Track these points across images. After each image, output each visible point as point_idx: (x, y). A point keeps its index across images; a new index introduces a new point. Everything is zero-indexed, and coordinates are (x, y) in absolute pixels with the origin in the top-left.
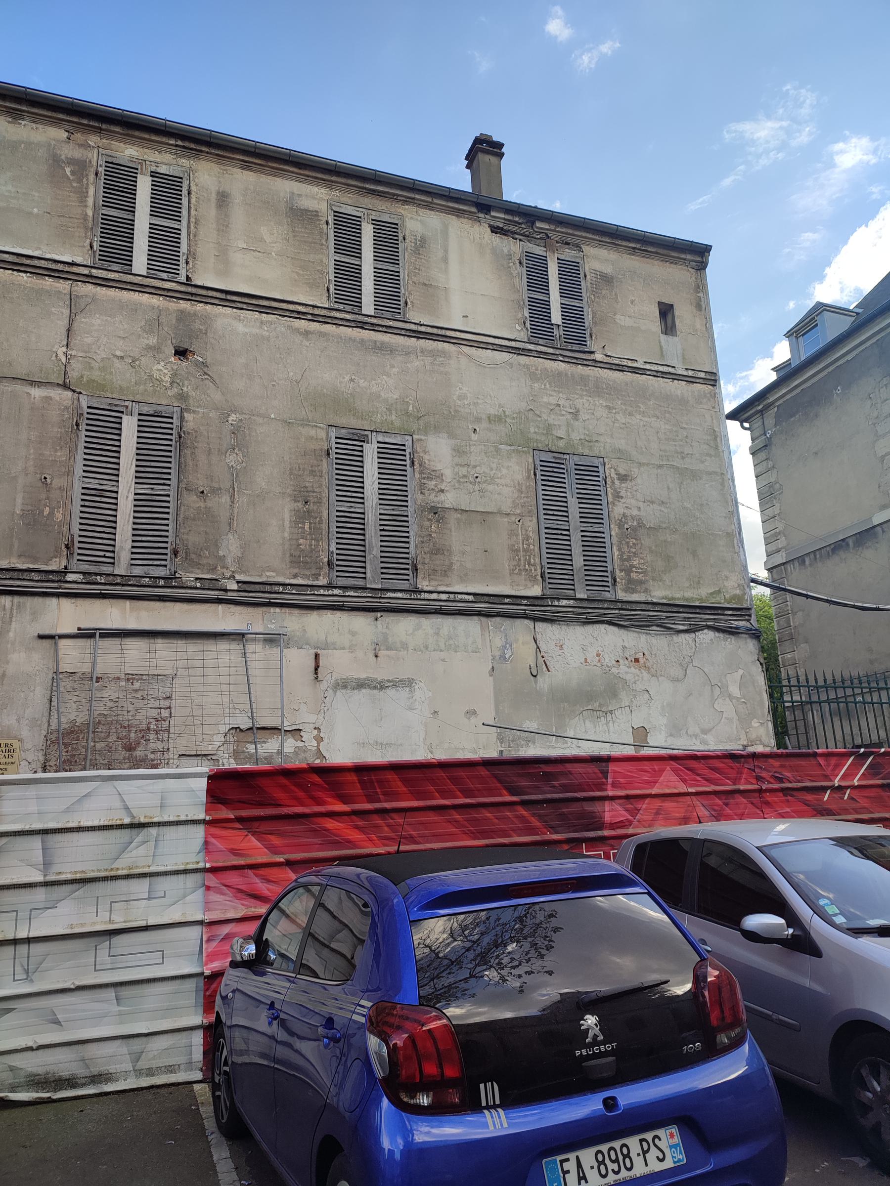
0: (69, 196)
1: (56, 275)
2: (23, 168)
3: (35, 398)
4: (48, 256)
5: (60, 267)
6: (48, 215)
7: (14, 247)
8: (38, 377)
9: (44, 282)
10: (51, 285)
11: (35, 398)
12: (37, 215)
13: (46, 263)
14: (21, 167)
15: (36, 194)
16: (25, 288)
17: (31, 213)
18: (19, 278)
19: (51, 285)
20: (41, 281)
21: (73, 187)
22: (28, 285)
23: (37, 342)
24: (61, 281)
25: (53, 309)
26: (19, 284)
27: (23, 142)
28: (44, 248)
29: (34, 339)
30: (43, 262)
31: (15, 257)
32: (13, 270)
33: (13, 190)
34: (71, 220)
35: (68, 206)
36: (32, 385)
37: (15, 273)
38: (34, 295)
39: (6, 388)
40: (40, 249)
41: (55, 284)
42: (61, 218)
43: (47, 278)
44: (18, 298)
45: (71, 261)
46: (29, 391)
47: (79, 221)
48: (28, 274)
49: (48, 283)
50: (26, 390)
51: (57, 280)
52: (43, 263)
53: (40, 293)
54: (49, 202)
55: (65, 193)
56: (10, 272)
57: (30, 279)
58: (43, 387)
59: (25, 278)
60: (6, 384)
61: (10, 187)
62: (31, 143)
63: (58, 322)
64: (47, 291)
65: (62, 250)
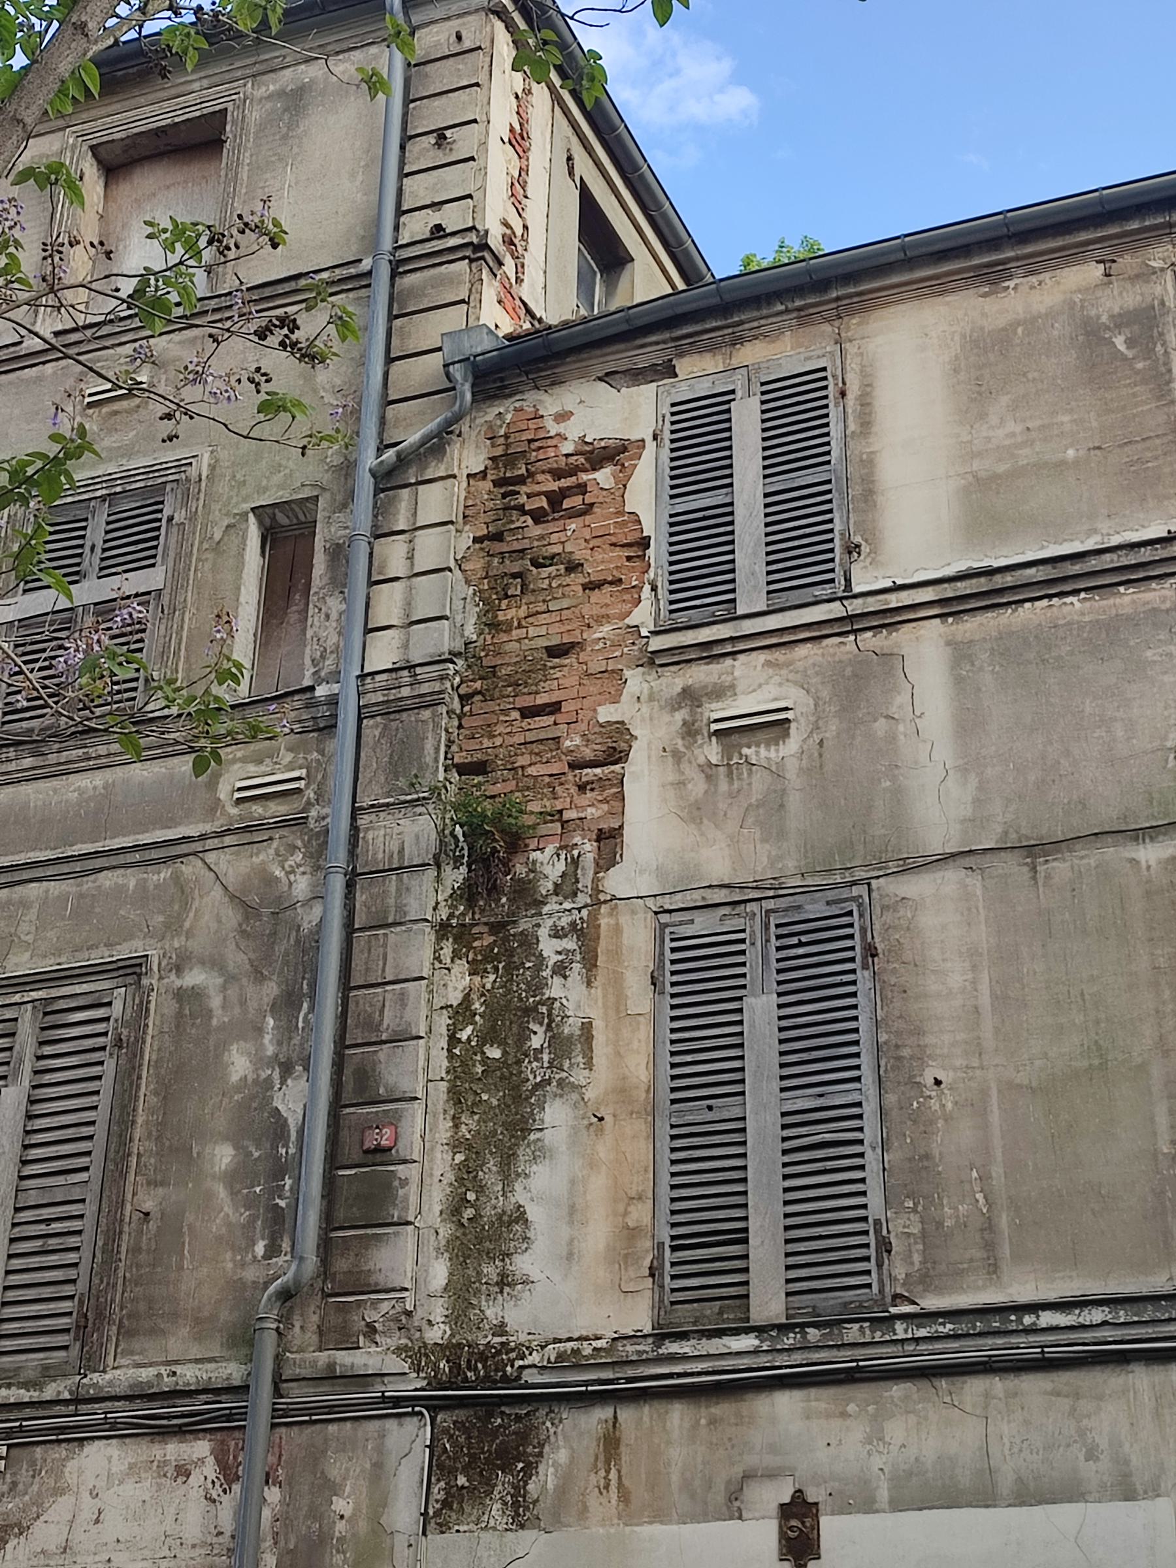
0: (1134, 395)
1: (1141, 575)
2: (1030, 376)
3: (1149, 867)
4: (1115, 541)
5: (1145, 555)
6: (1097, 452)
7: (1043, 548)
8: (1147, 818)
9: (1118, 601)
10: (1134, 602)
11: (1149, 867)
12: (1076, 462)
13: (1114, 556)
14: (1024, 375)
15: (1066, 418)
16: (1081, 627)
17: (1063, 463)
18: (1066, 609)
19: (1134, 602)
20: (1111, 601)
21: (1138, 372)
22: (1087, 619)
23: (1129, 739)
24: (1154, 585)
25: (1149, 653)
26: (1069, 624)
27: (1018, 323)
28: (1104, 526)
29: (1120, 733)
30: (1107, 557)
31: (1049, 567)
32: (1050, 596)
33: (1018, 428)
34: (1148, 443)
35: (1134, 416)
36: (1136, 839)
37: (1055, 601)
38: (1104, 635)
39: (1085, 861)
40: (1095, 531)
41: (1141, 596)
42: (1126, 449)
43: (1122, 589)
44: (1072, 653)
45: (1165, 534)
46: (1134, 855)
47: (1165, 439)
48: (1083, 595)
49: (1127, 599)
50: (1127, 855)
51: (1143, 586)
52: (1108, 561)
53: (1112, 627)
54: (1095, 424)
55: (1124, 392)
56: (1045, 602)
57: (1088, 604)
58: (1161, 838)
59: (1078, 605)
60: (1083, 853)
61: (1011, 427)
62: (1034, 319)
63: (1166, 678)
64: (1128, 618)
65: (1141, 516)
